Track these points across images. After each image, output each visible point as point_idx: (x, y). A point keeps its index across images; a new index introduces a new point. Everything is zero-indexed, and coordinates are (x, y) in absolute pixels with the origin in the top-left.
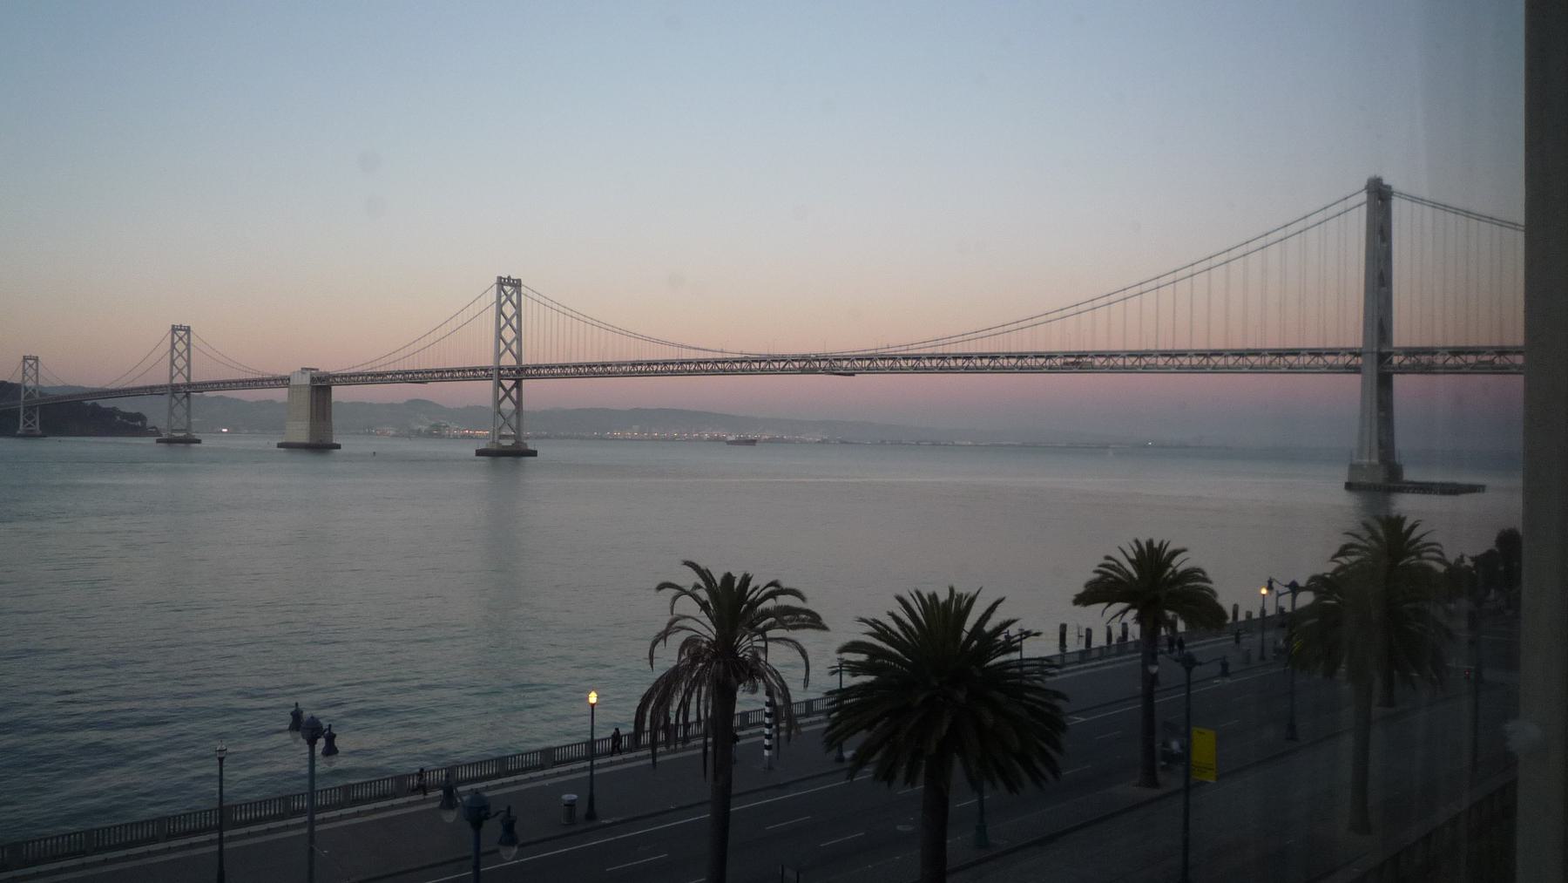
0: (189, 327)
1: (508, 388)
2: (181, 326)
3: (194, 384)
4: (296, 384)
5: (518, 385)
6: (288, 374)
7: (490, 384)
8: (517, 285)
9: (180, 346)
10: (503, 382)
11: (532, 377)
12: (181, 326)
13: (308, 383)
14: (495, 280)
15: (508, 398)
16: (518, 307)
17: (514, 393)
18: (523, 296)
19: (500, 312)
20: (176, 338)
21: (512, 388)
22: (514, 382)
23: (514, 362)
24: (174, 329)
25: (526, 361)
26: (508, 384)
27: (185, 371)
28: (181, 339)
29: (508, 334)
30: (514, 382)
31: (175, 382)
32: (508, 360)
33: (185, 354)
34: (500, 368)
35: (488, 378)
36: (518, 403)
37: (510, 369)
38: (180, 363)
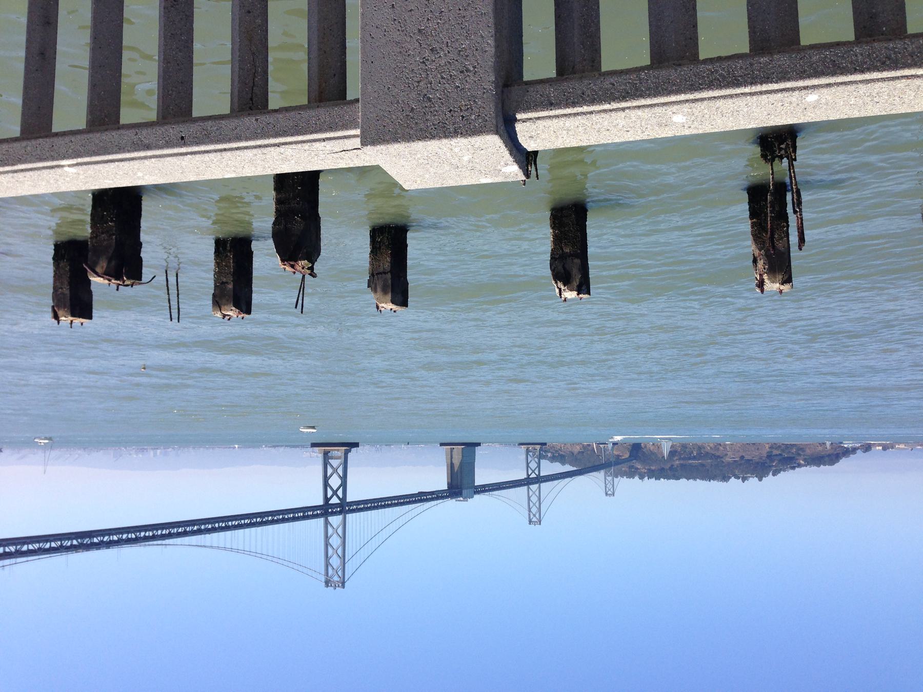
2: (535, 525)
3: (524, 485)
4: (471, 490)
5: (327, 499)
6: (476, 497)
9: (534, 510)
10: (339, 502)
12: (535, 525)
13: (463, 491)
14: (346, 584)
16: (327, 564)
17: (330, 493)
18: (323, 572)
20: (537, 516)
22: (329, 503)
23: (330, 519)
25: (321, 520)
26: (335, 500)
27: (531, 493)
29: (335, 541)
30: (329, 503)
31: (537, 485)
32: (335, 520)
33: (531, 505)
34: (340, 513)
36: (326, 484)
37: (333, 514)
38: (534, 499)
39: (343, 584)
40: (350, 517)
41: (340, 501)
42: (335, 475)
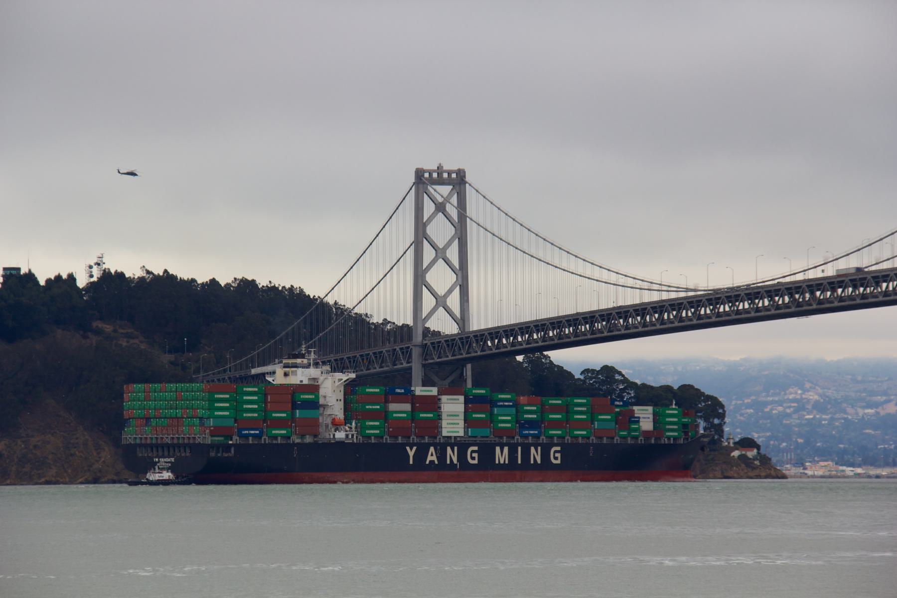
0: (461, 174)
2: (440, 171)
12: (440, 171)
20: (429, 208)
24: (422, 180)
28: (440, 208)
33: (453, 254)
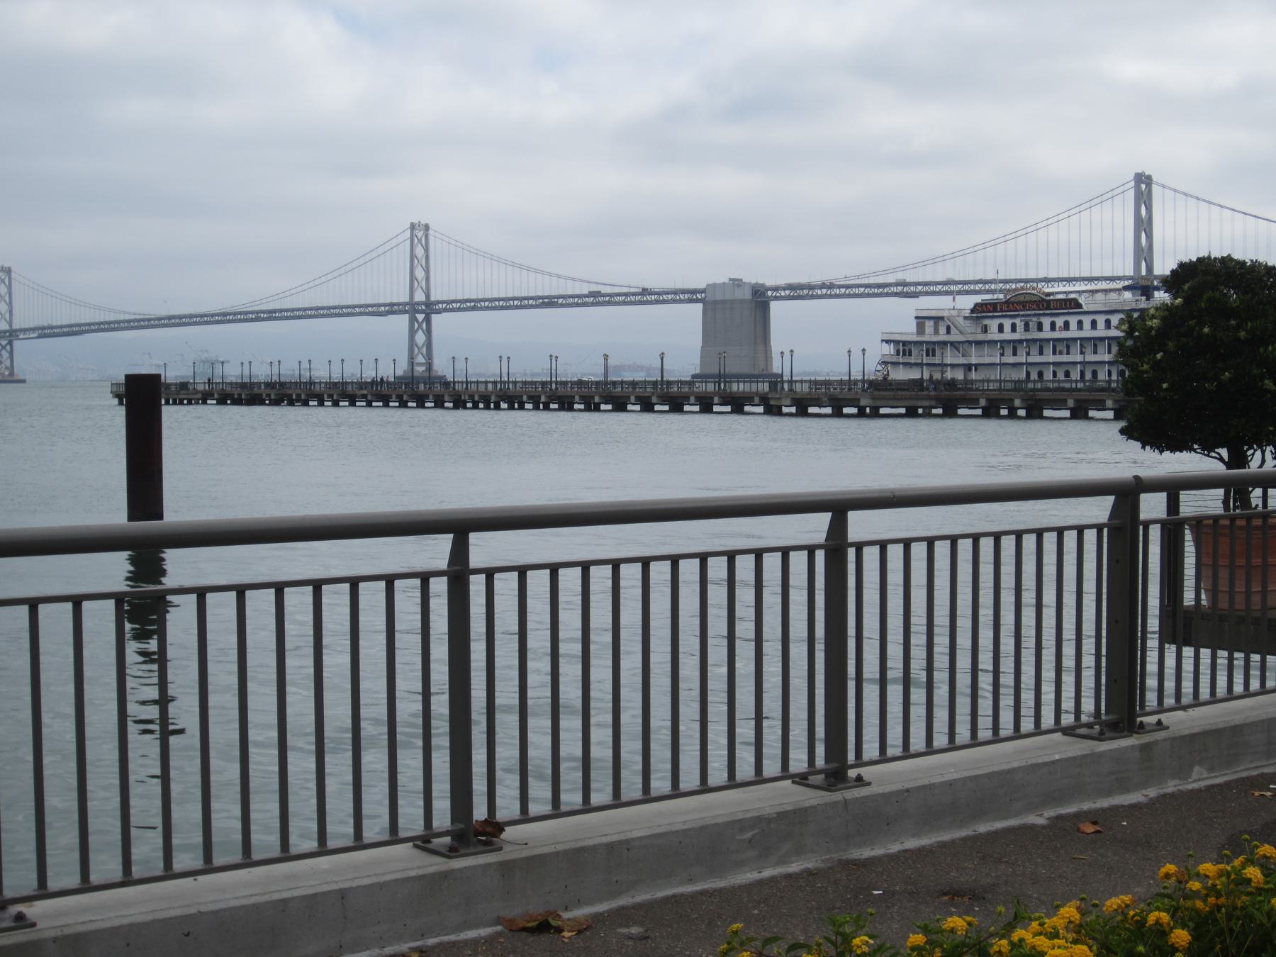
1: (420, 321)
7: (406, 317)
8: (427, 227)
10: (417, 315)
11: (439, 312)
15: (420, 331)
19: (413, 256)
21: (423, 321)
23: (423, 299)
25: (433, 298)
32: (420, 297)
34: (418, 304)
35: (406, 312)
39: (413, 227)
40: (404, 298)
41: (416, 317)
42: (420, 345)
